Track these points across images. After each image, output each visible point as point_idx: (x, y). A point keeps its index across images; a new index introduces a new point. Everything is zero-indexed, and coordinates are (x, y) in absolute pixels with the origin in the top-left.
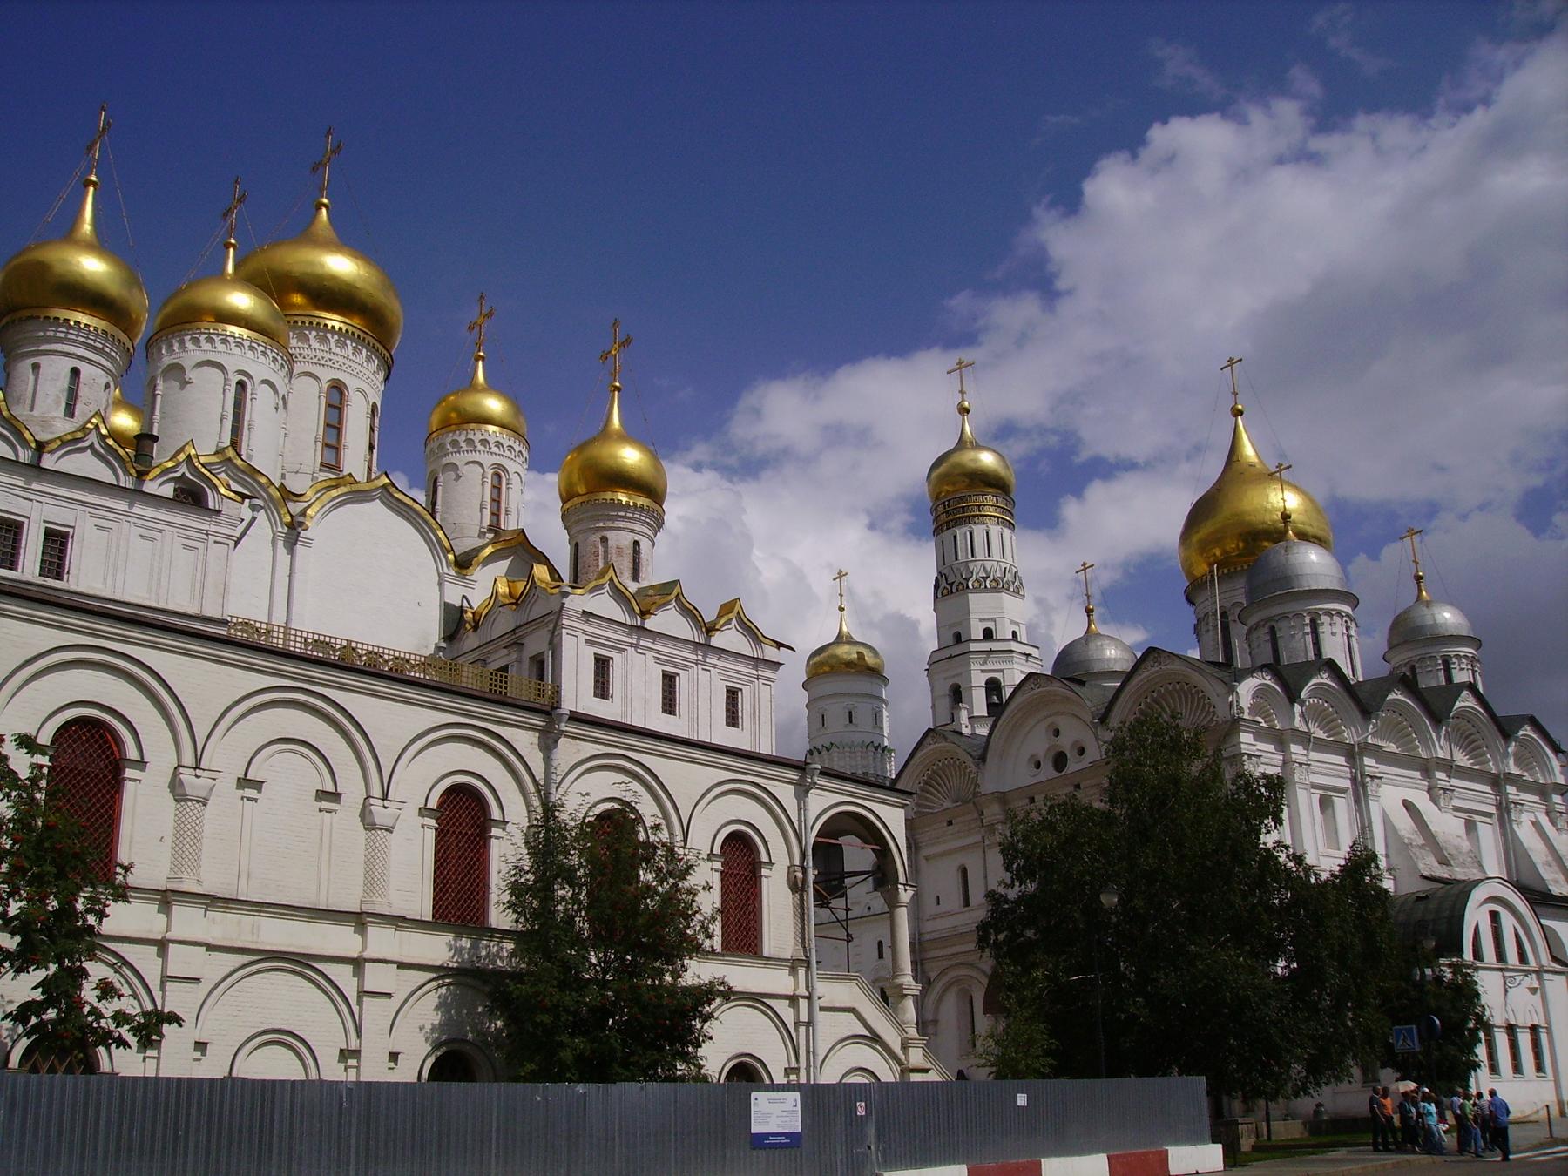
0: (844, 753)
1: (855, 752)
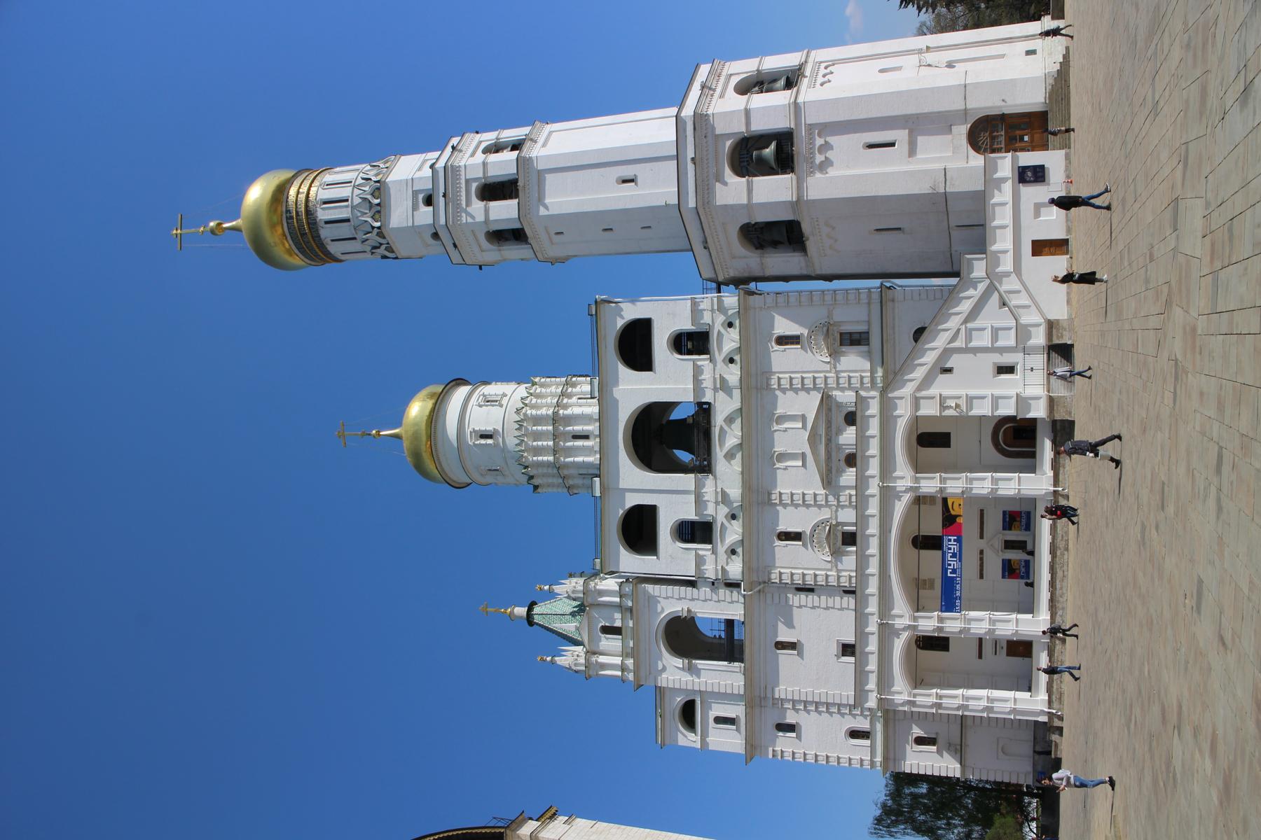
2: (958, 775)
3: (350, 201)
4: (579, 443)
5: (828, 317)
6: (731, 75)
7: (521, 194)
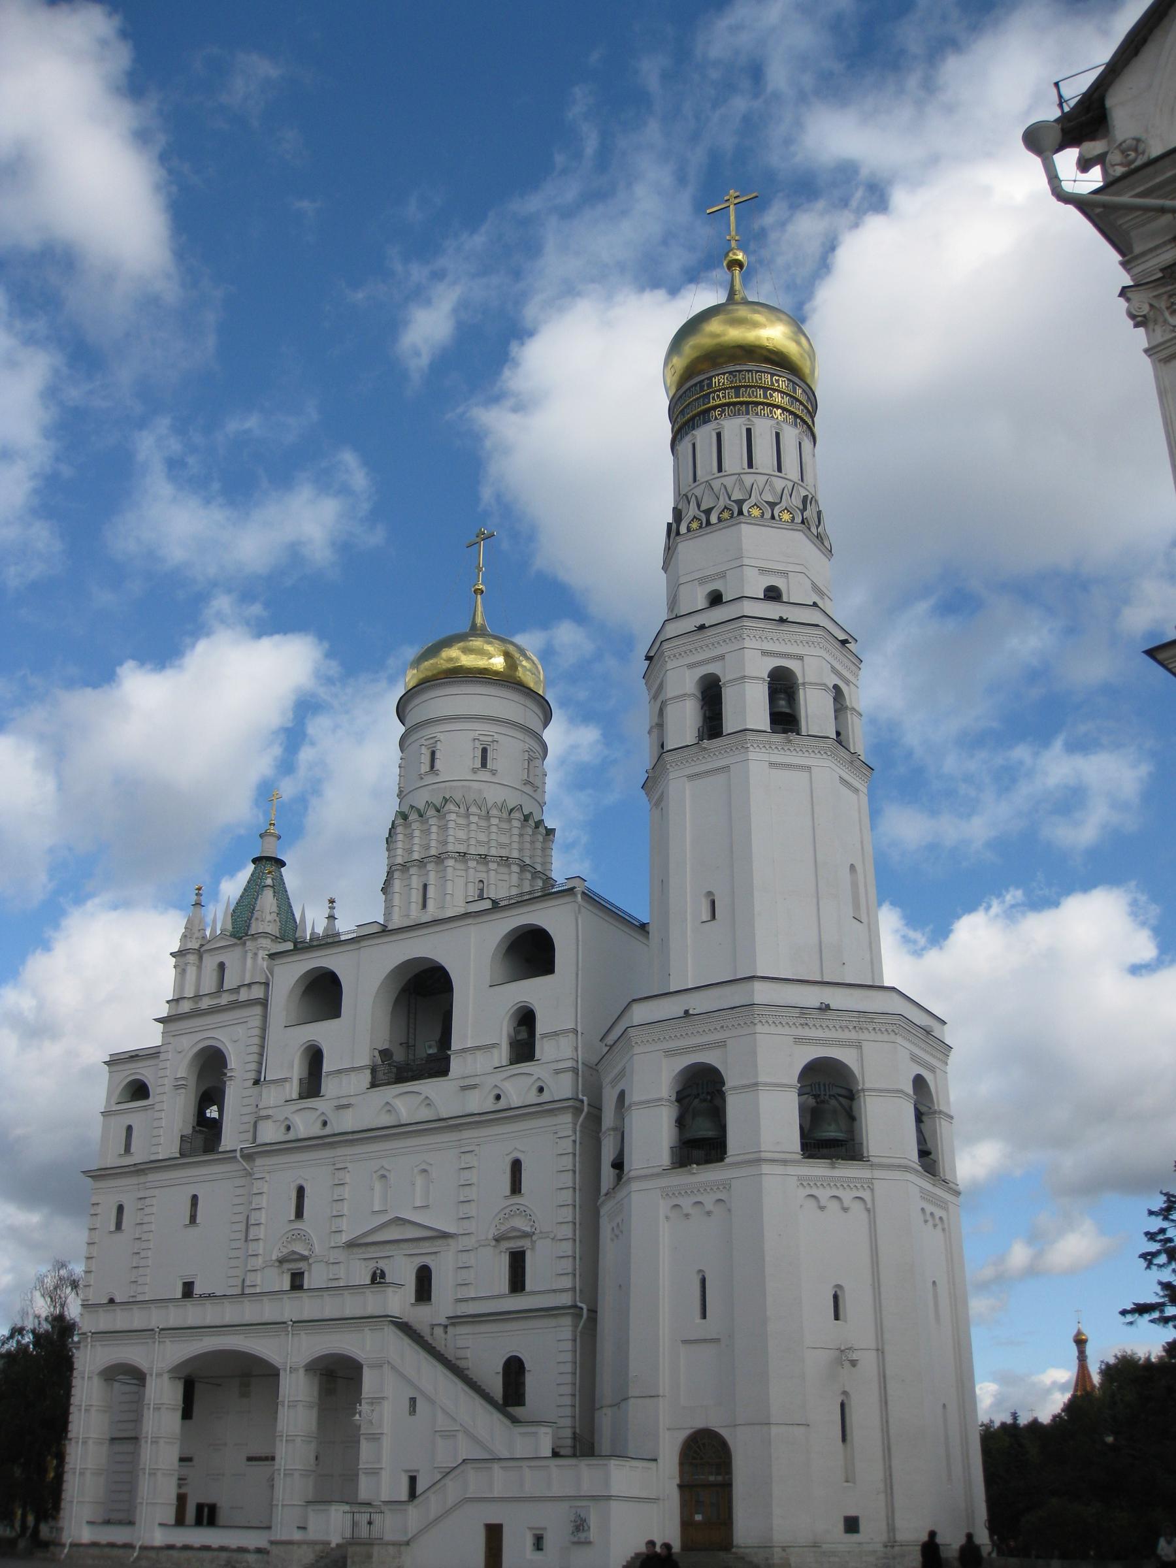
0: (467, 815)
1: (488, 817)
3: (721, 474)
4: (416, 896)
5: (541, 1232)
6: (858, 1045)
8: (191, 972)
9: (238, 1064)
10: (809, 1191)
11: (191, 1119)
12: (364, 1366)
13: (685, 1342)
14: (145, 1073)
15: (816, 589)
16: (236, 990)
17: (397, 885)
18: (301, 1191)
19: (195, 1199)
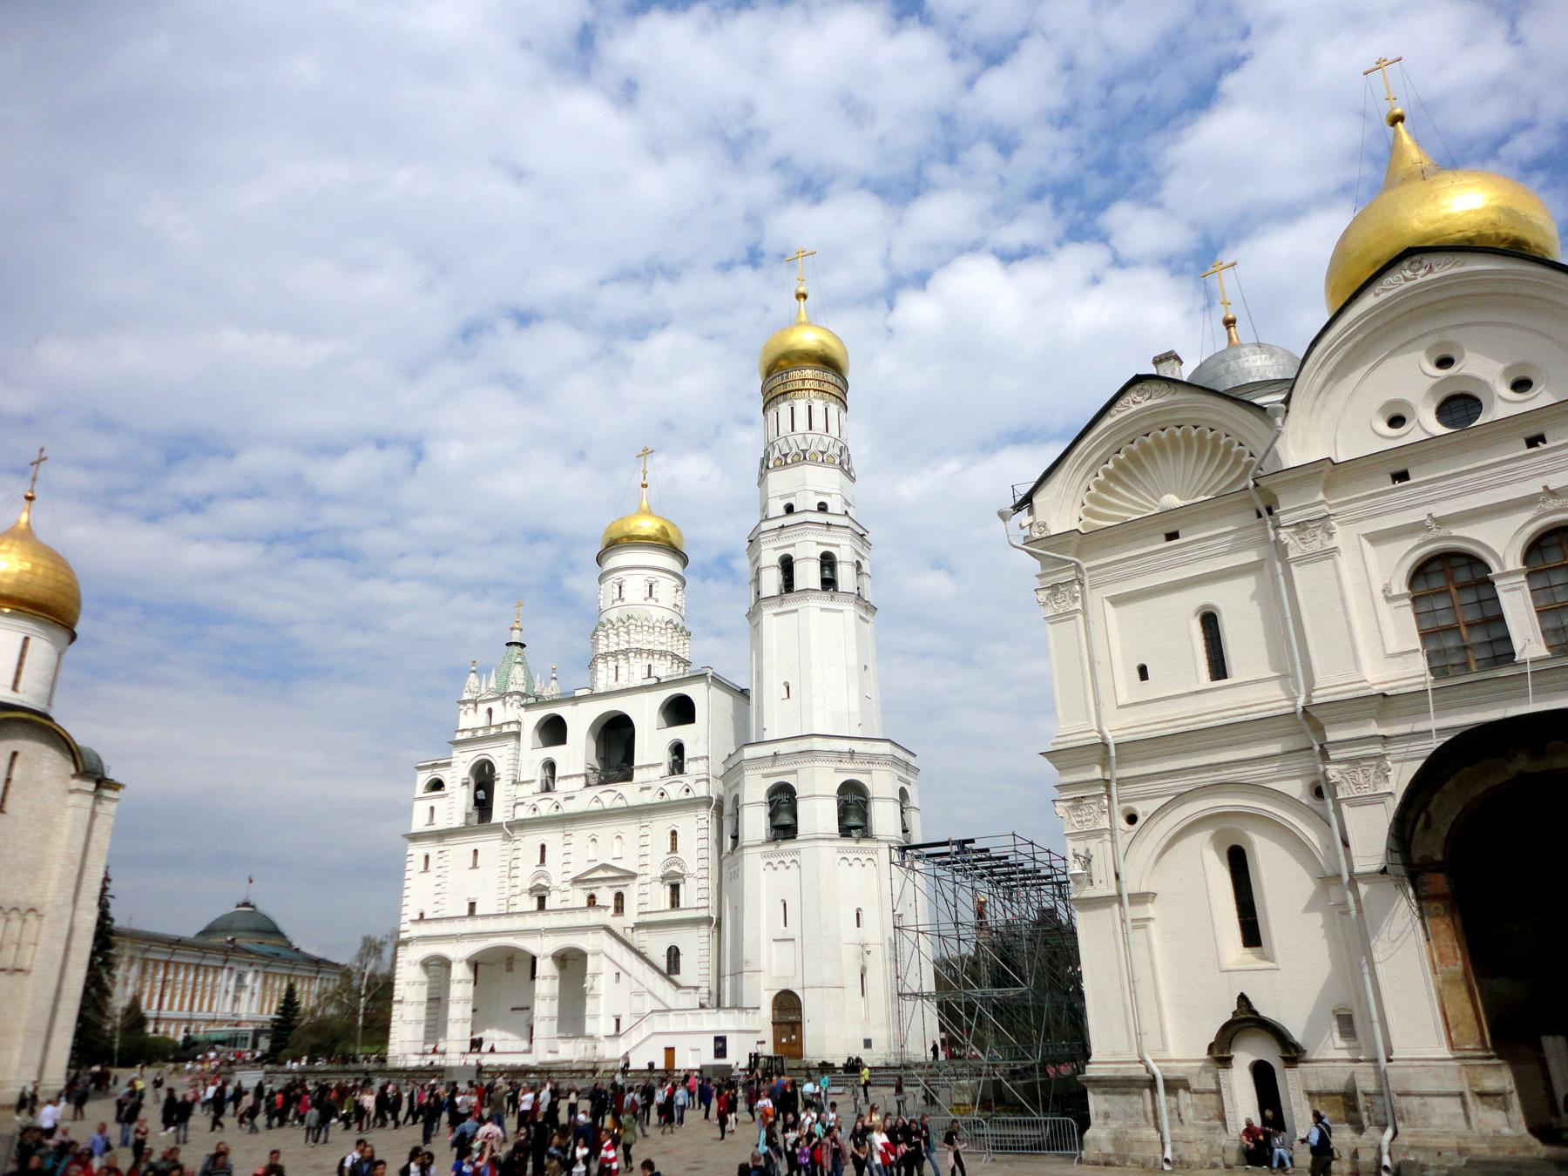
1: (653, 628)
2: (395, 998)
7: (778, 600)
8: (471, 712)
9: (501, 769)
10: (843, 855)
11: (472, 802)
12: (589, 956)
13: (775, 940)
14: (443, 774)
15: (847, 503)
16: (500, 726)
17: (600, 665)
18: (543, 847)
19: (476, 851)
